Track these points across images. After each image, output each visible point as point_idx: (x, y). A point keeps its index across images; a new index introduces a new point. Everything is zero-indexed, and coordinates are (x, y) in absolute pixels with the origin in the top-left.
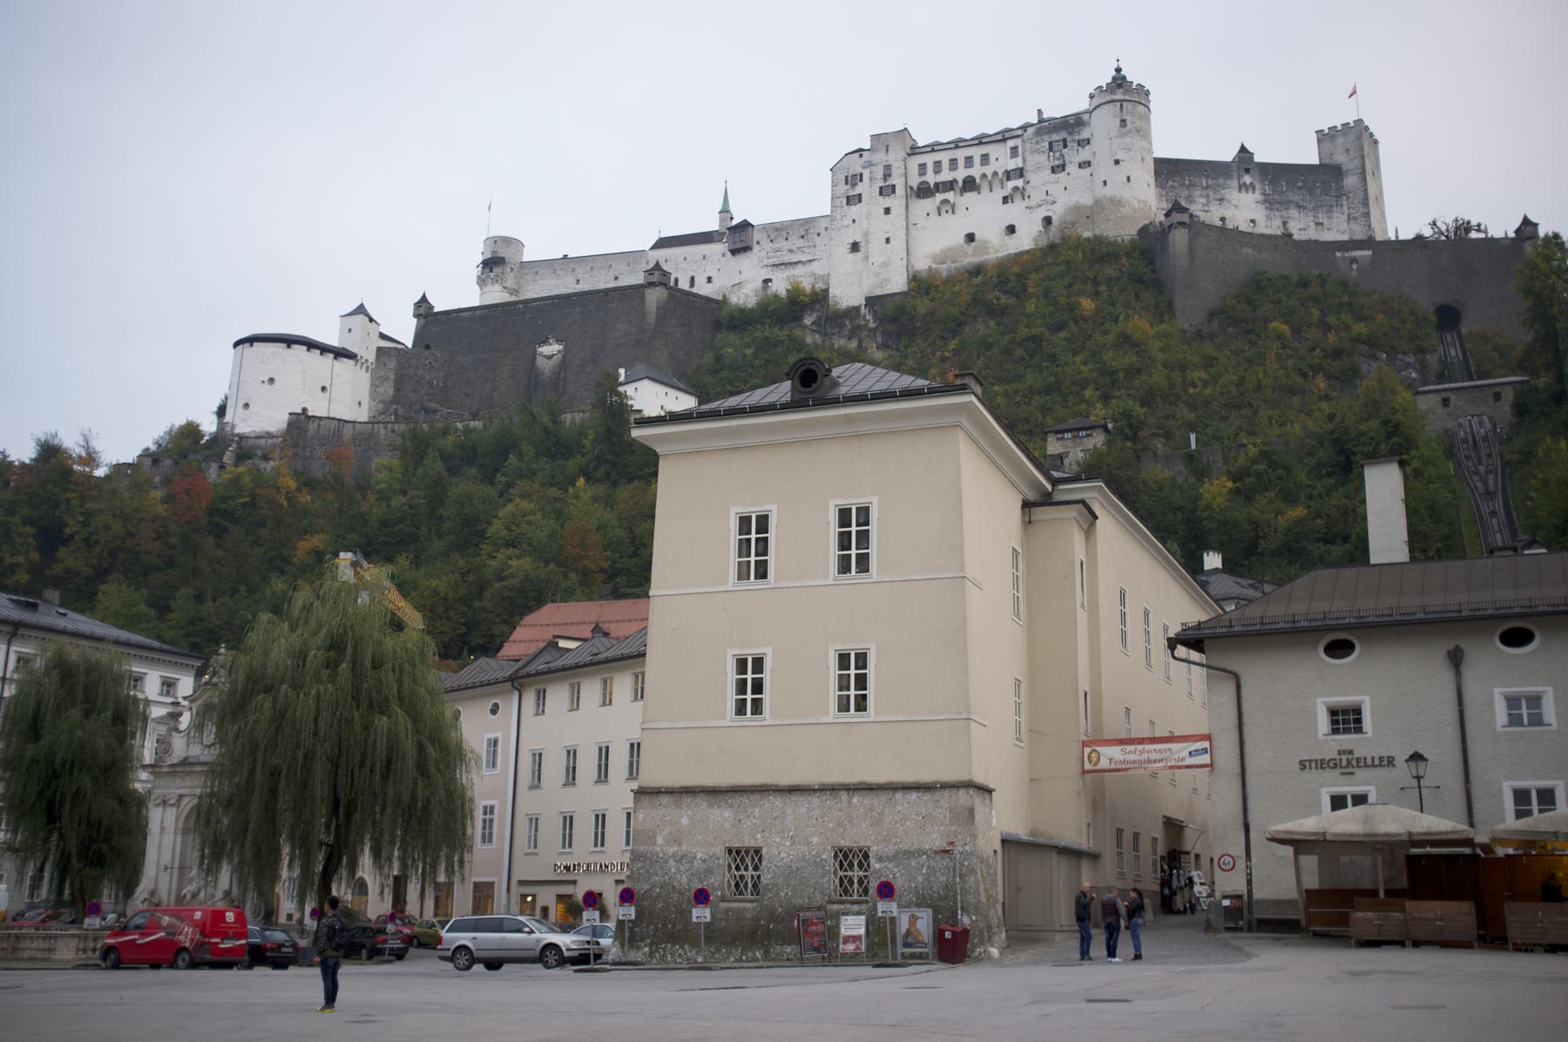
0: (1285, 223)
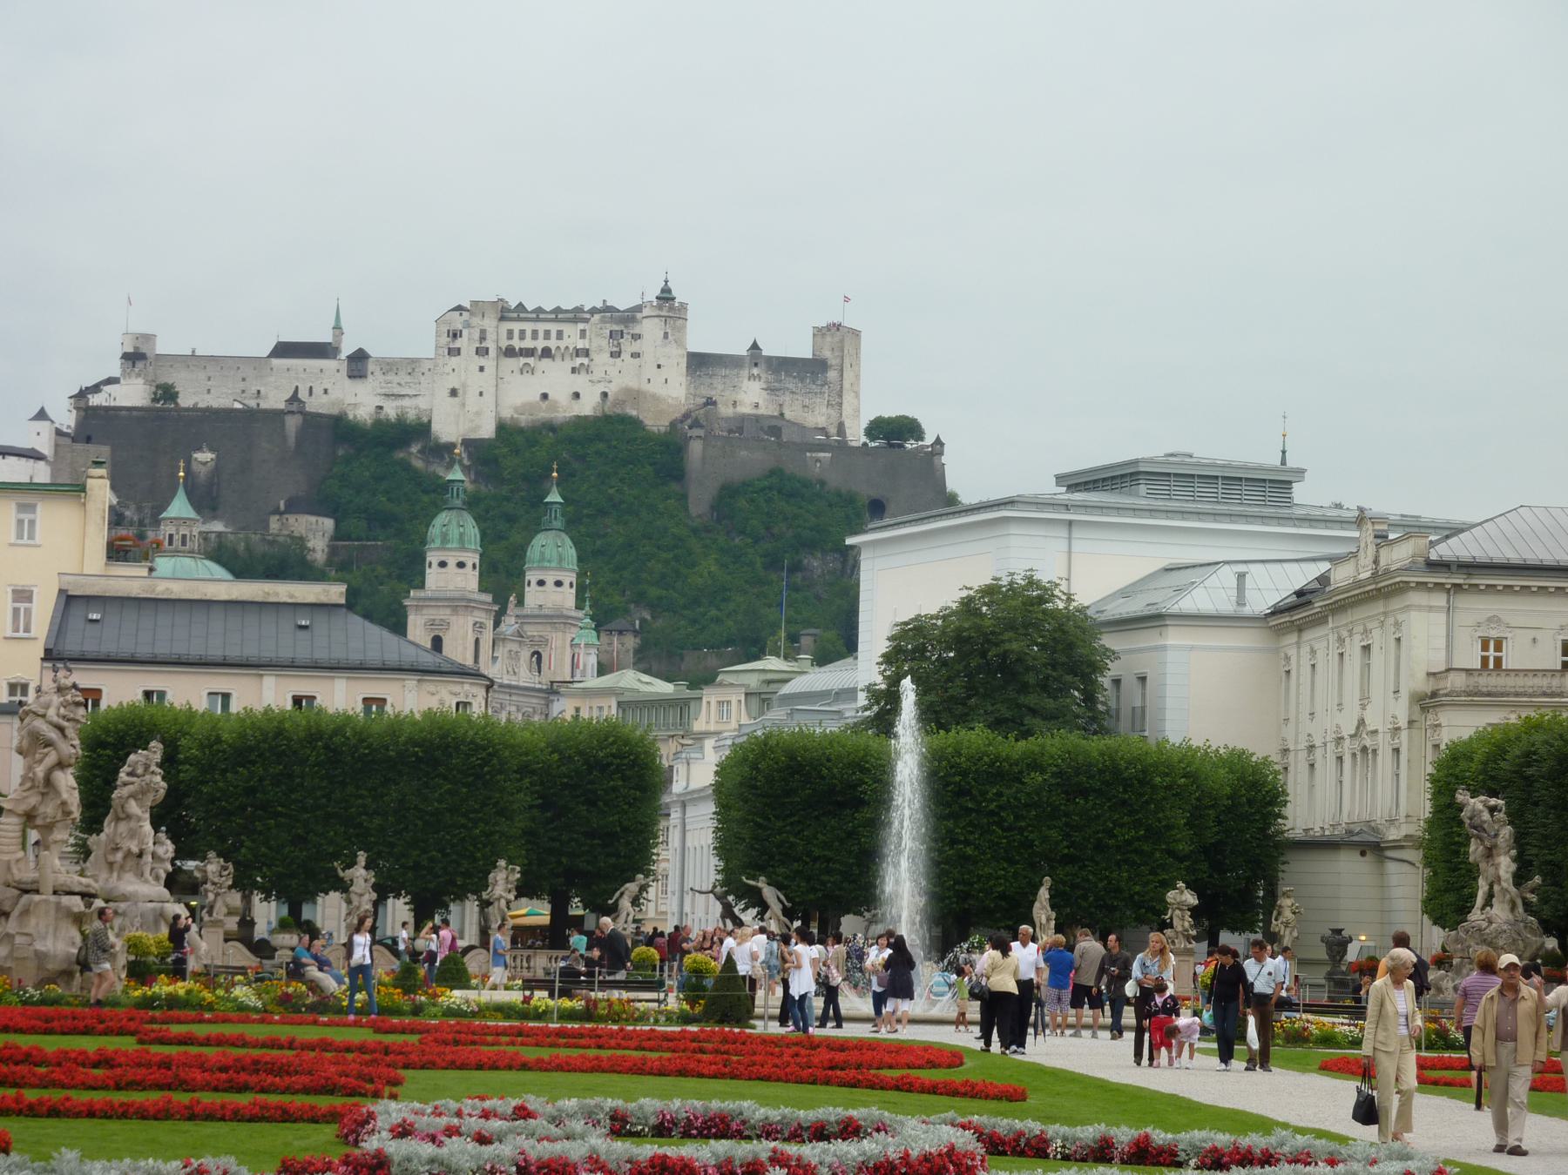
0: (781, 405)
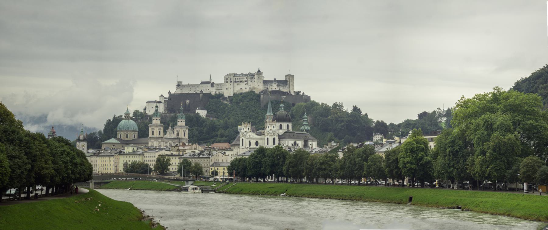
0: (280, 88)
